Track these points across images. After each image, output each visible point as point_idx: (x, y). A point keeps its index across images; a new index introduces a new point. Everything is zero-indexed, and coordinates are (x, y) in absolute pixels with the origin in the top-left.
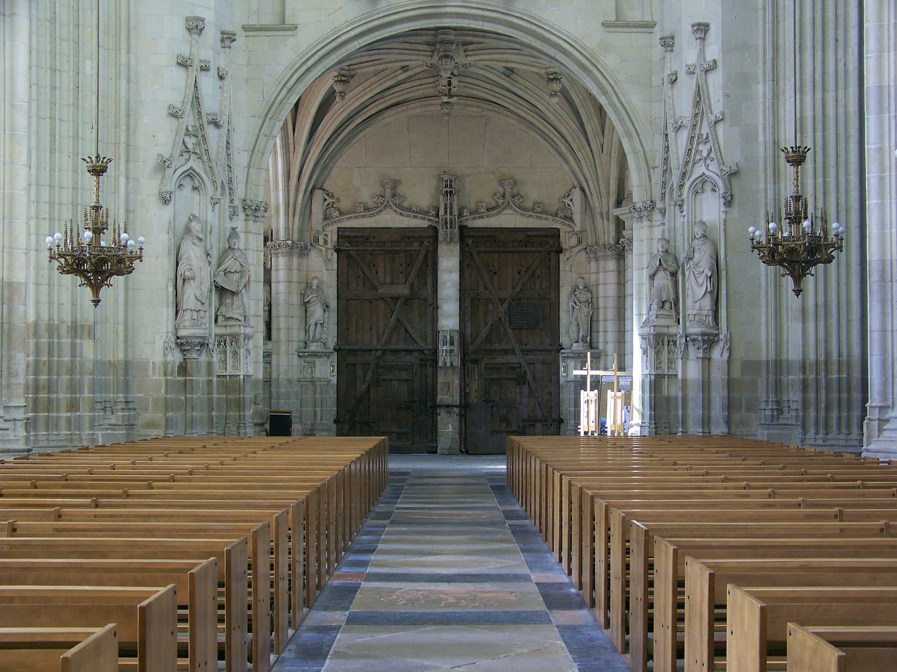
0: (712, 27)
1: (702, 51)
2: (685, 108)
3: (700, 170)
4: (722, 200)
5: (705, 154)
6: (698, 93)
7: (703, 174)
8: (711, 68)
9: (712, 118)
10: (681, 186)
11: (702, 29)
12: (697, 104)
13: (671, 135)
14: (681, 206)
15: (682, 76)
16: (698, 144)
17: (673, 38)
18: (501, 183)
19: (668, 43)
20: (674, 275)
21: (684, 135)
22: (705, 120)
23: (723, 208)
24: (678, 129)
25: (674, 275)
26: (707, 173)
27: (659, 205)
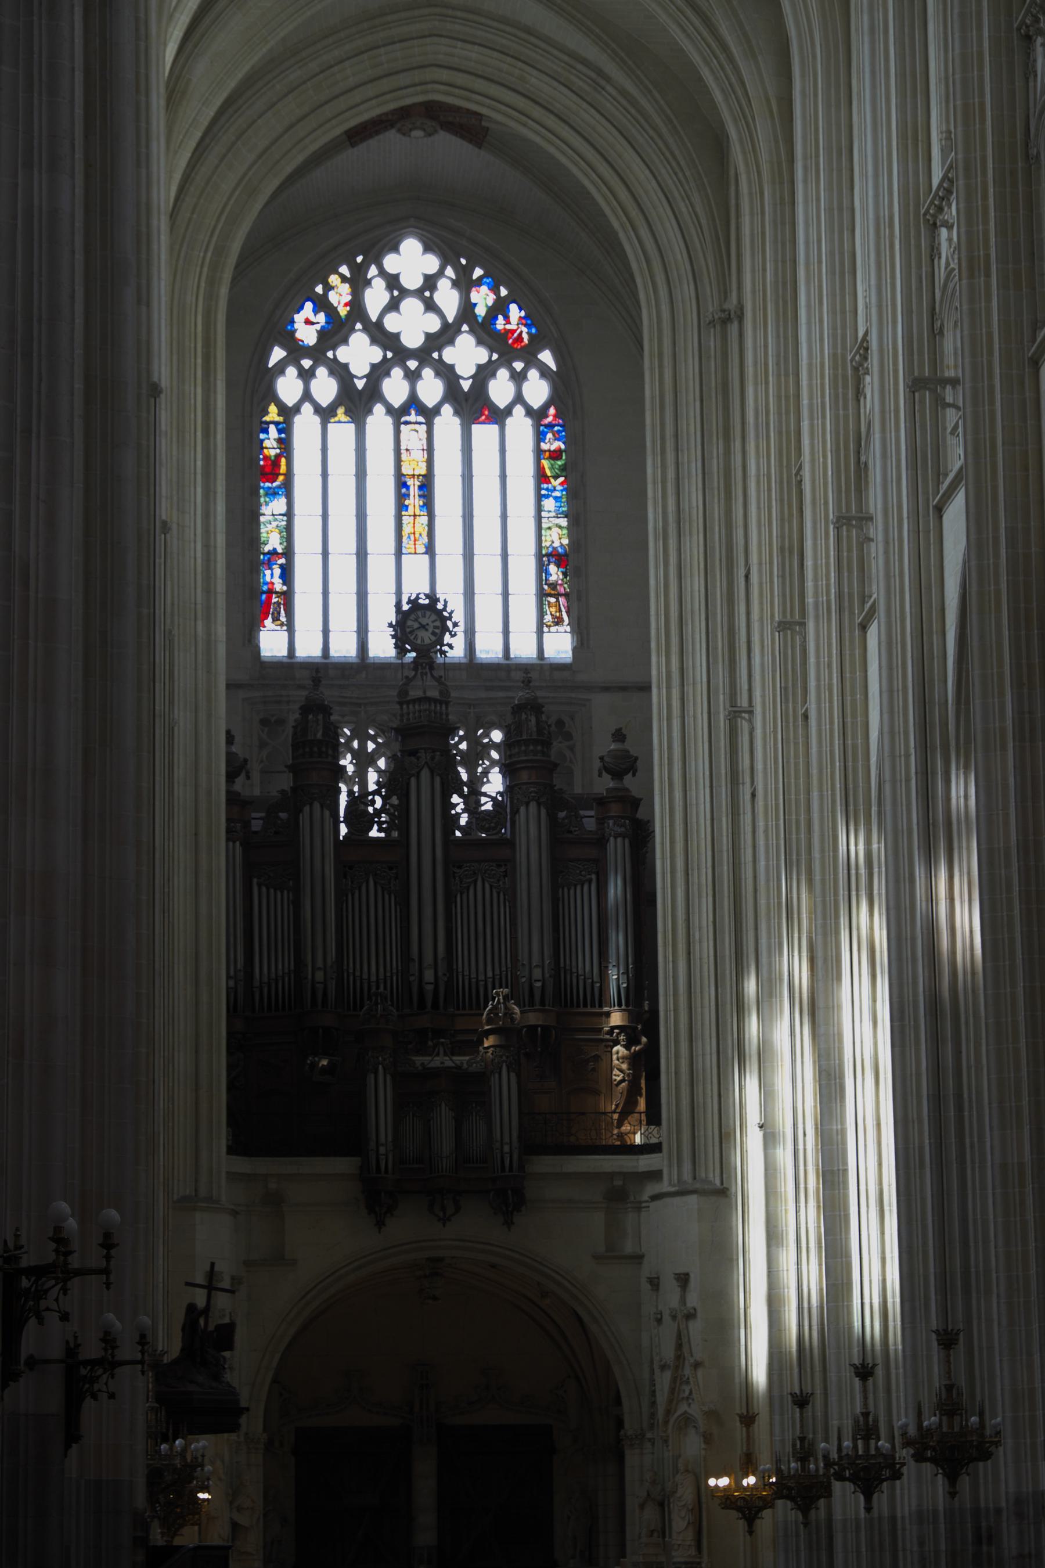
0: (692, 1276)
1: (683, 1300)
2: (668, 1353)
3: (683, 1408)
4: (702, 1439)
5: (687, 1393)
6: (679, 1336)
7: (686, 1412)
8: (691, 1316)
9: (692, 1361)
10: (666, 1423)
11: (683, 1280)
12: (679, 1346)
13: (657, 1371)
14: (666, 1441)
15: (666, 1318)
16: (681, 1384)
17: (658, 1278)
19: (655, 1283)
20: (661, 1505)
21: (668, 1375)
22: (687, 1362)
23: (703, 1446)
24: (663, 1367)
25: (661, 1505)
26: (689, 1411)
27: (649, 1435)
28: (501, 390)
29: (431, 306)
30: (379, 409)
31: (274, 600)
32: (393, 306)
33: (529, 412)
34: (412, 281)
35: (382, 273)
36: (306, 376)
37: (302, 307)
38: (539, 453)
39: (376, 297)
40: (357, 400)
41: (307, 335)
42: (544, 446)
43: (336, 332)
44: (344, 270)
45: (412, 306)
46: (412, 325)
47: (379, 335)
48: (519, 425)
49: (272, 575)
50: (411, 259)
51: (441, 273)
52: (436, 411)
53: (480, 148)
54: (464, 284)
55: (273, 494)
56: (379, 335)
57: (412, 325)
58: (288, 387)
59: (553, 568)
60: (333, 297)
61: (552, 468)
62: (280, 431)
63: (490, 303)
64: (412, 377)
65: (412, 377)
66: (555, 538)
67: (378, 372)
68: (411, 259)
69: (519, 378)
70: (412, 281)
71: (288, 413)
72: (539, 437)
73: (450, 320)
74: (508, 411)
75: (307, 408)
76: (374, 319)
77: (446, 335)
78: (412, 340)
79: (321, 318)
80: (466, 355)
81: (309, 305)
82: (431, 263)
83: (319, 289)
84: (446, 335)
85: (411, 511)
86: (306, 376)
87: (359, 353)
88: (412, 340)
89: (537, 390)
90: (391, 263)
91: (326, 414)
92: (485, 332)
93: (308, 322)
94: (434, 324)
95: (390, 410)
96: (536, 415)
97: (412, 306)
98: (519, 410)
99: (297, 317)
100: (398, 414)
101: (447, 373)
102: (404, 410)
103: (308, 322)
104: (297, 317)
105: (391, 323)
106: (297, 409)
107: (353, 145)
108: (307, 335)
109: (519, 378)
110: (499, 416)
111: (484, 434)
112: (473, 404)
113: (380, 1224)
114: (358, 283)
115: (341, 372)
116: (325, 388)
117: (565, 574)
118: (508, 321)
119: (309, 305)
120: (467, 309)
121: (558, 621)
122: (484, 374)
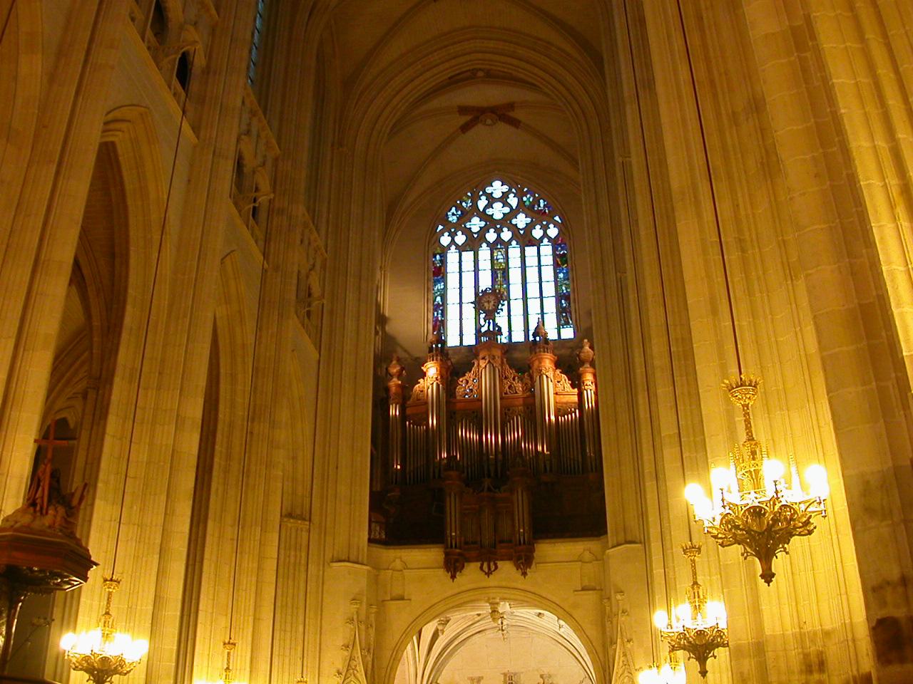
18: (542, 676)
28: (537, 233)
29: (506, 204)
30: (484, 245)
31: (438, 323)
32: (489, 205)
33: (550, 239)
34: (497, 195)
35: (485, 193)
36: (453, 235)
37: (451, 209)
38: (555, 255)
39: (482, 203)
40: (473, 243)
41: (453, 219)
42: (558, 253)
43: (465, 216)
44: (469, 194)
45: (498, 205)
46: (498, 211)
47: (483, 216)
48: (547, 250)
49: (437, 314)
50: (497, 188)
51: (510, 191)
52: (510, 242)
53: (517, 128)
54: (519, 195)
55: (439, 282)
56: (483, 216)
57: (498, 211)
58: (445, 240)
59: (563, 301)
60: (464, 204)
61: (561, 261)
62: (441, 257)
63: (531, 200)
64: (499, 232)
65: (499, 232)
66: (564, 288)
67: (484, 230)
68: (497, 188)
69: (545, 228)
70: (497, 195)
71: (444, 251)
72: (554, 250)
73: (514, 208)
74: (541, 240)
75: (453, 247)
76: (481, 210)
77: (513, 213)
78: (498, 216)
79: (459, 213)
80: (521, 221)
81: (453, 210)
82: (505, 188)
83: (458, 202)
84: (513, 213)
85: (499, 283)
86: (453, 235)
87: (476, 224)
88: (498, 216)
89: (553, 232)
90: (489, 190)
91: (461, 249)
92: (529, 210)
93: (453, 214)
94: (507, 210)
95: (488, 244)
96: (555, 243)
97: (498, 205)
98: (546, 241)
99: (449, 213)
100: (493, 246)
101: (514, 229)
102: (496, 242)
103: (453, 214)
104: (449, 213)
105: (489, 212)
106: (449, 247)
107: (464, 133)
108: (453, 219)
109: (545, 228)
110: (537, 243)
111: (531, 251)
112: (525, 239)
113: (453, 577)
114: (475, 199)
115: (468, 232)
116: (460, 239)
117: (569, 304)
118: (539, 206)
119: (454, 209)
120: (520, 202)
121: (567, 323)
122: (529, 227)
